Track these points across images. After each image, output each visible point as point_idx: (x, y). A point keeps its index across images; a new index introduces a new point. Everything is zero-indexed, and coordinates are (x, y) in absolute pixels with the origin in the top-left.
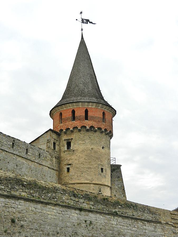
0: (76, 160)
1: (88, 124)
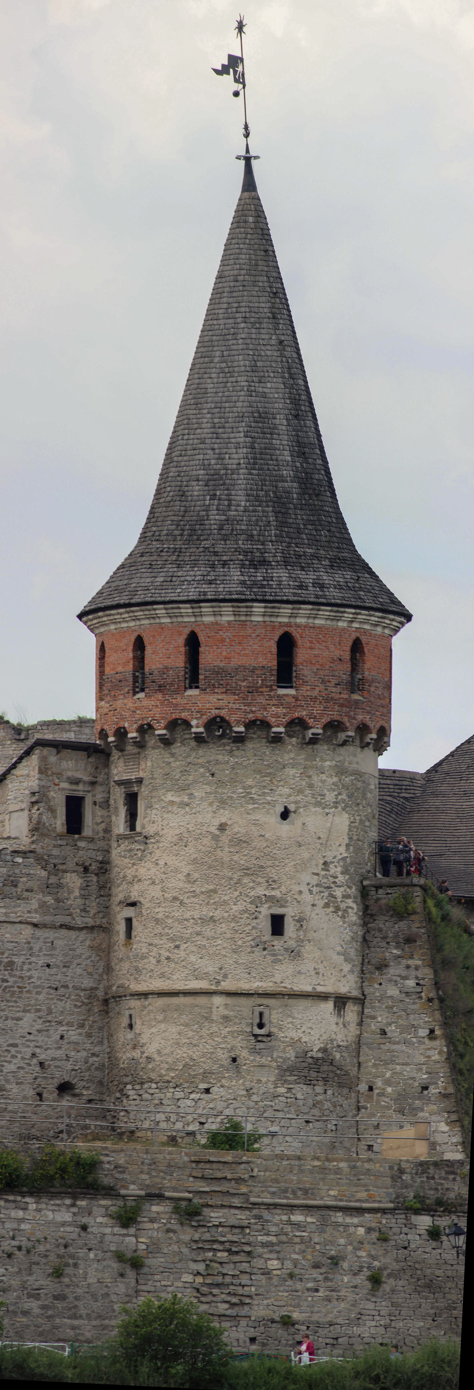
1: (199, 704)
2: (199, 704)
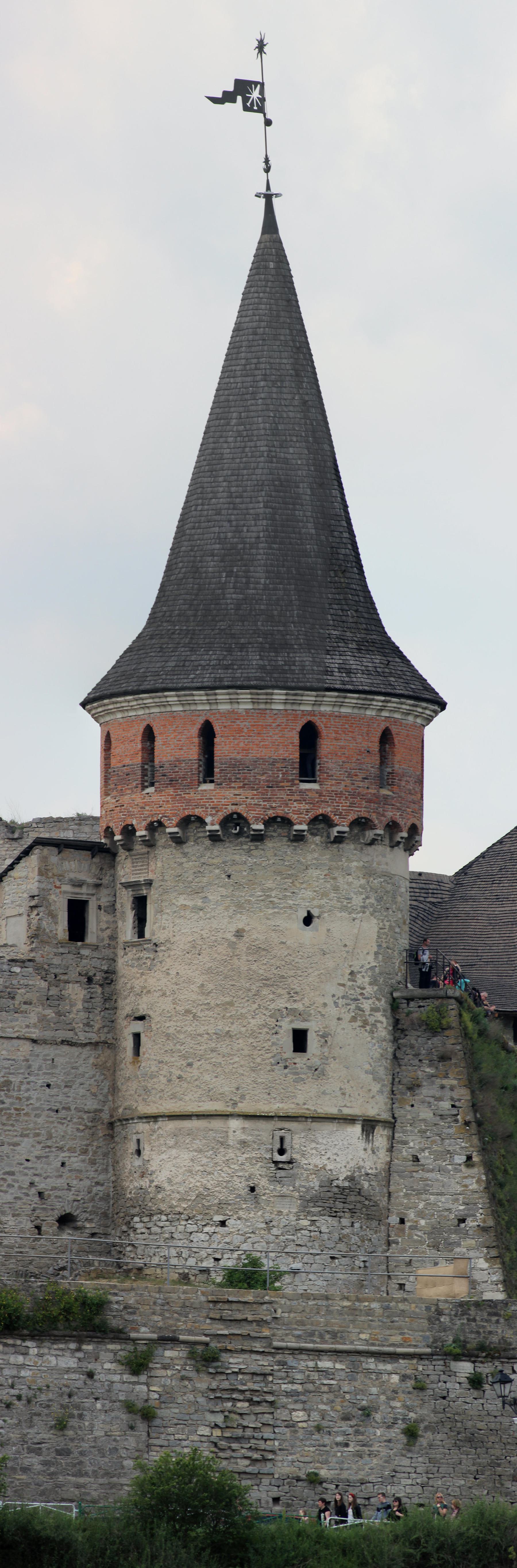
0: (164, 995)
1: (214, 800)
2: (214, 800)
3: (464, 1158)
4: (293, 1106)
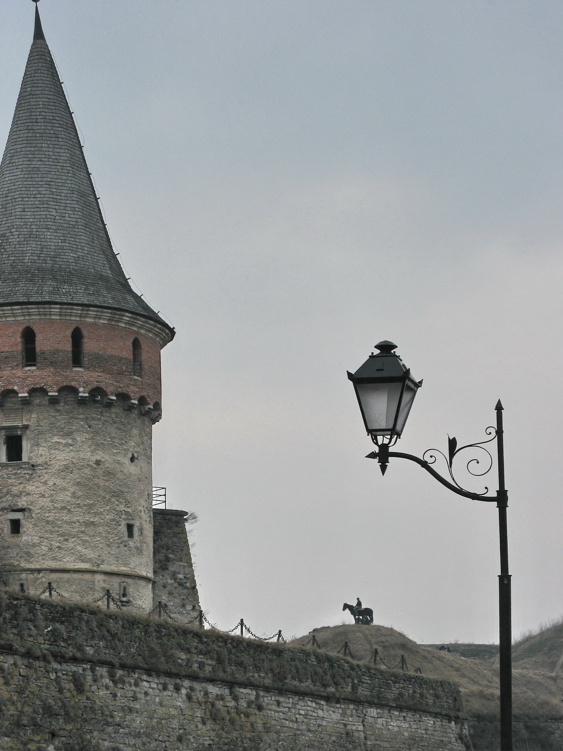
1: (84, 379)
2: (84, 379)
3: (192, 607)
4: (129, 569)
